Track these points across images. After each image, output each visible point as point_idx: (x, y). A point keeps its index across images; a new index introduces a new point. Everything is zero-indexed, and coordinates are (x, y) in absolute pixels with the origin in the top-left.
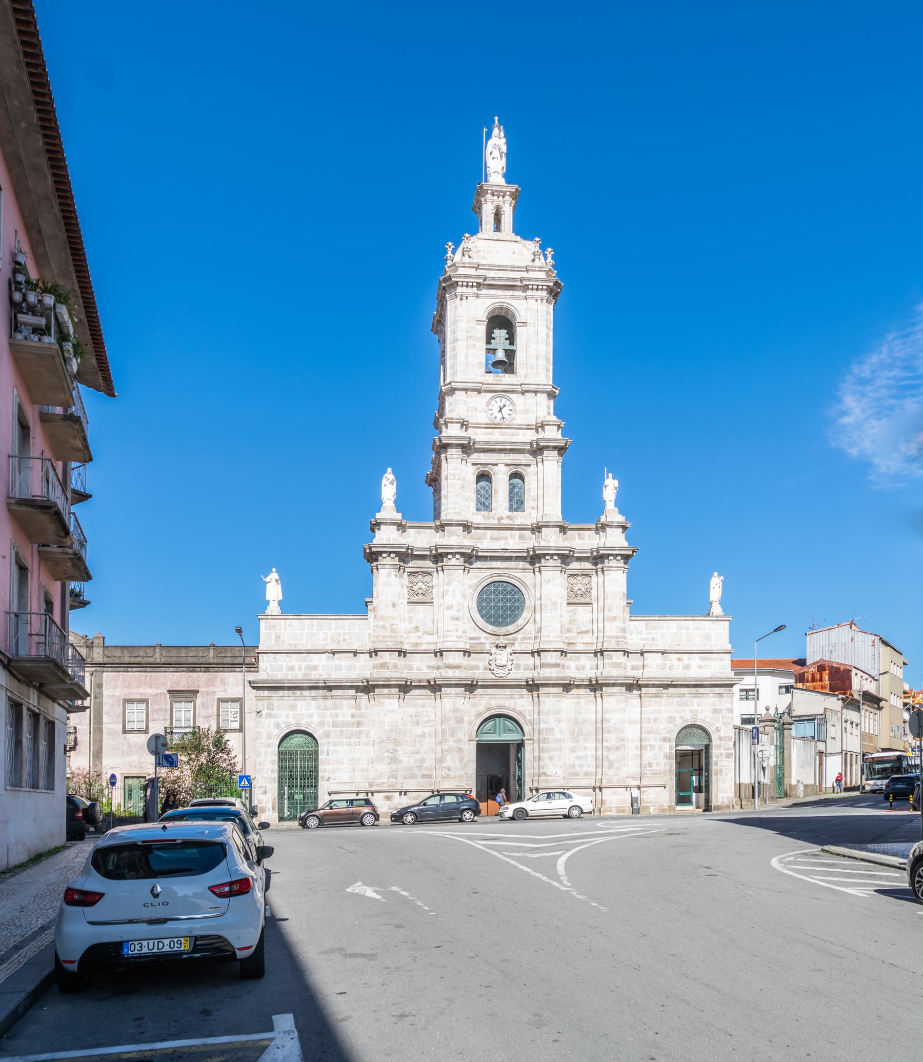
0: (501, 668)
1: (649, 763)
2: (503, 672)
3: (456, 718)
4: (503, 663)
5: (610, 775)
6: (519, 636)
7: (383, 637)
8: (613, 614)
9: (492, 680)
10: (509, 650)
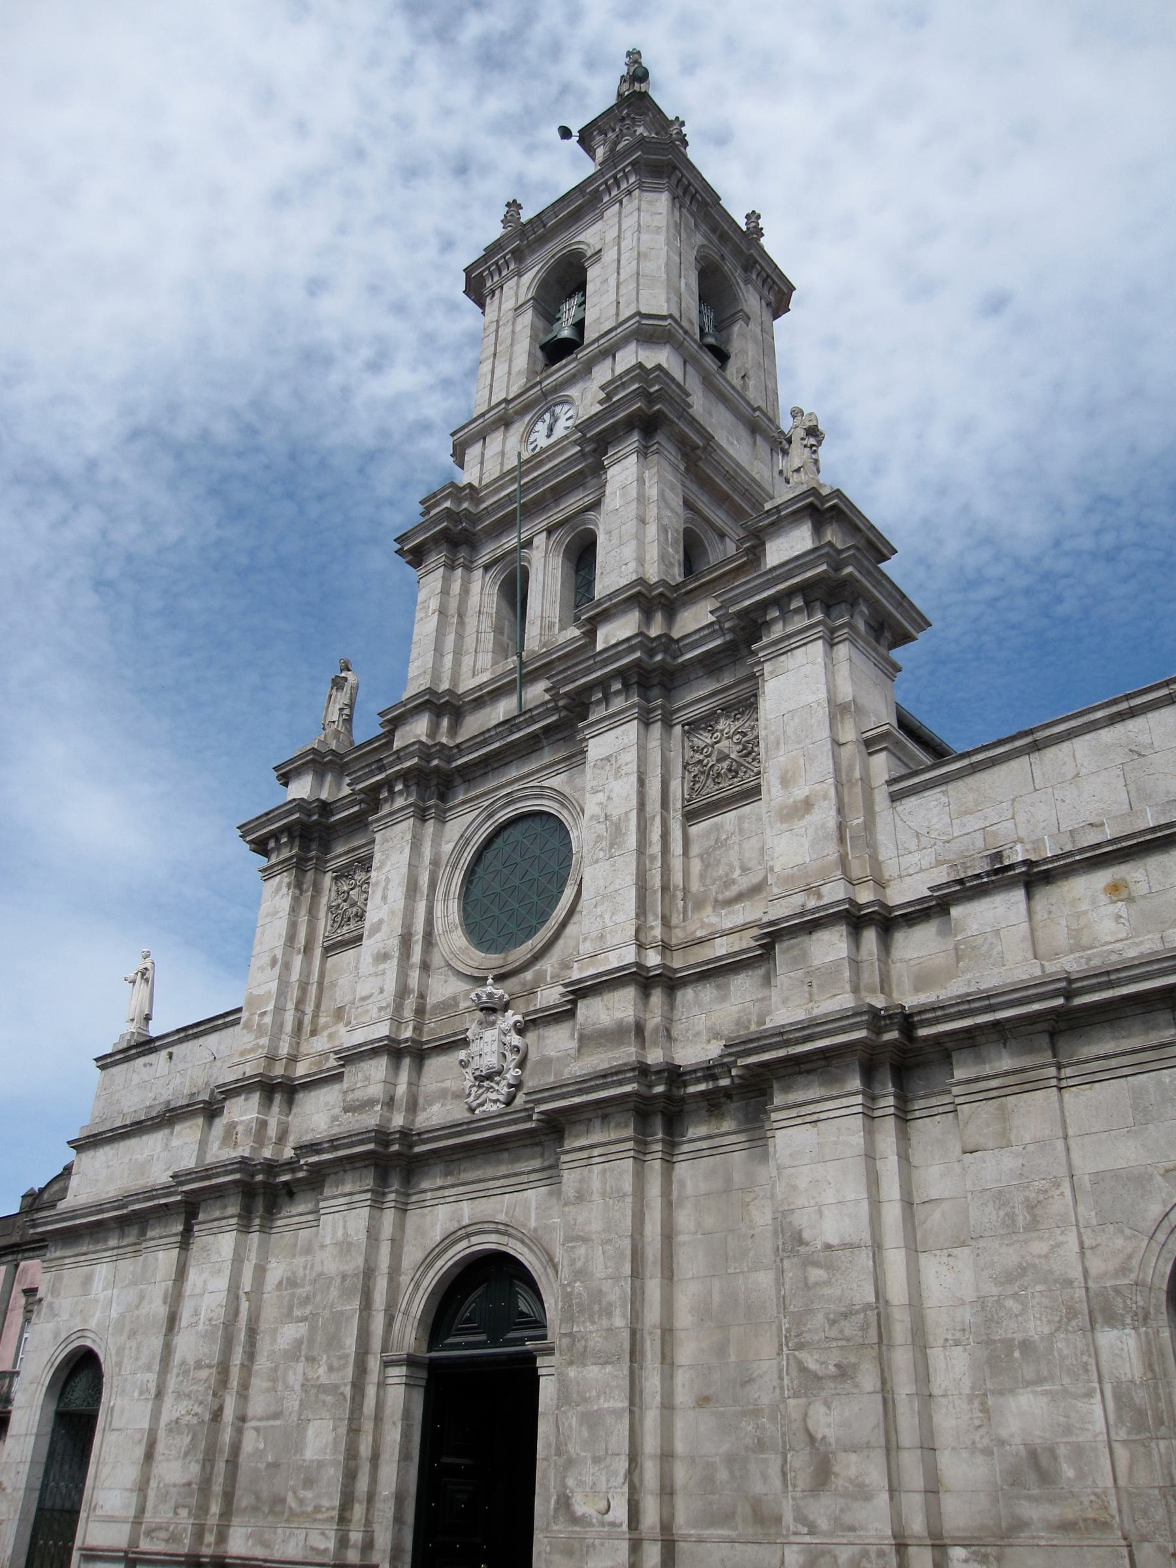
0: (486, 1084)
1: (1033, 1454)
2: (494, 1096)
3: (344, 1277)
4: (491, 1060)
5: (823, 1524)
6: (548, 965)
7: (242, 1054)
8: (800, 792)
9: (454, 1129)
10: (511, 1017)
